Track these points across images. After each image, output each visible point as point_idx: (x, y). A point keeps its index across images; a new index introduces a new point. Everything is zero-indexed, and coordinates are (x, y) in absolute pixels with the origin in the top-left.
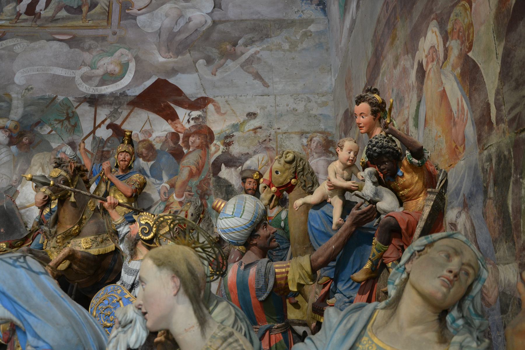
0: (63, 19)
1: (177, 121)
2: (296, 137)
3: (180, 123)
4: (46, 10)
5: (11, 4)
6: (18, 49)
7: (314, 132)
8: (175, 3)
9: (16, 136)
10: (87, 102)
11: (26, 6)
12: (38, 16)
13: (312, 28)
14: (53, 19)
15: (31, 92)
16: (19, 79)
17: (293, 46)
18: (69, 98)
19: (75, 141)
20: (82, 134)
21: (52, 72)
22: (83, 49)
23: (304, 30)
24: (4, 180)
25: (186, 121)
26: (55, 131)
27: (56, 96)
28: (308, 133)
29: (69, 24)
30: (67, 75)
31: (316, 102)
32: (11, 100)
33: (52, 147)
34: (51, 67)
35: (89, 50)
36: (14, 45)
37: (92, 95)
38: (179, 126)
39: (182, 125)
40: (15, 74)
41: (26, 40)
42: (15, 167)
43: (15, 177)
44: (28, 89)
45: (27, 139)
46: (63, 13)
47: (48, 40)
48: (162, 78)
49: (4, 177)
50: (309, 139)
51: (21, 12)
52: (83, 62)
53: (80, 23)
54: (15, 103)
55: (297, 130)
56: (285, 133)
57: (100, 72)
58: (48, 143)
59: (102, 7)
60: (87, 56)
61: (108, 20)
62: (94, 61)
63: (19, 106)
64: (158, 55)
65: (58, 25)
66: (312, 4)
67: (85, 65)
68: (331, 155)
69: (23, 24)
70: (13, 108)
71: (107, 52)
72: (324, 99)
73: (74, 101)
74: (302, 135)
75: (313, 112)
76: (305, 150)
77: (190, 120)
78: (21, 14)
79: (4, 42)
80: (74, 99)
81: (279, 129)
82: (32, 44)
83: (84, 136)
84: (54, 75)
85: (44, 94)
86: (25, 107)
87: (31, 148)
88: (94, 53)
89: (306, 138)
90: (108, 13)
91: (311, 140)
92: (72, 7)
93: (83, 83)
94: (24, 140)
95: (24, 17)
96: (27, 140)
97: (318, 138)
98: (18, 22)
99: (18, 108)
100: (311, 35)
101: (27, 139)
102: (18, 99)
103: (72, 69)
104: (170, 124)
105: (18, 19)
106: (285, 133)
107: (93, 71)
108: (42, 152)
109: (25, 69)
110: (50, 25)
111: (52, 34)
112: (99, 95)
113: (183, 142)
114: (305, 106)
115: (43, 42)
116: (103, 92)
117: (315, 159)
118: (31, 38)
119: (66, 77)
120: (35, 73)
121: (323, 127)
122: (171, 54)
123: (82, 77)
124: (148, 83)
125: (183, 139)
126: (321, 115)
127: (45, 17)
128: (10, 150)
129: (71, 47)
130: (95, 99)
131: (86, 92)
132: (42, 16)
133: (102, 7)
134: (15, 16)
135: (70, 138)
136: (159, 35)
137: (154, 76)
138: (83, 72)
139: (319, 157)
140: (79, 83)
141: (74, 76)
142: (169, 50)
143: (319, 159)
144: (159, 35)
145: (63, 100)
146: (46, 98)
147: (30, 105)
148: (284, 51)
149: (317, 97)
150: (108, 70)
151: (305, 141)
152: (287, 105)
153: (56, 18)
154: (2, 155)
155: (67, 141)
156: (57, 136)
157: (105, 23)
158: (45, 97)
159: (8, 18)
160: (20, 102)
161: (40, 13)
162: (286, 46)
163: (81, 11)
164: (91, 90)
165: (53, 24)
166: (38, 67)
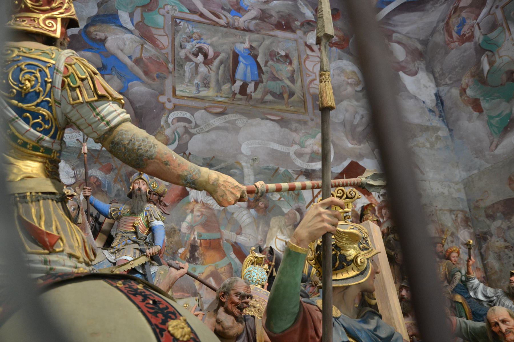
0: (270, 102)
1: (371, 196)
2: (448, 214)
3: (373, 198)
4: (255, 93)
5: (227, 84)
6: (239, 123)
7: (458, 210)
8: (350, 102)
9: (252, 201)
10: (304, 175)
11: (239, 88)
12: (250, 97)
13: (440, 133)
14: (263, 101)
15: (257, 162)
16: (245, 149)
17: (432, 146)
18: (288, 170)
19: (301, 208)
20: (305, 203)
21: (271, 147)
22: (291, 129)
23: (436, 134)
24: (251, 240)
25: (377, 197)
26: (284, 198)
27: (278, 168)
28: (454, 211)
29: (277, 107)
30: (282, 150)
31: (454, 188)
32: (242, 168)
33: (284, 212)
34: (269, 142)
35: (296, 131)
36: (236, 120)
37: (306, 170)
38: (373, 200)
39: (375, 200)
40: (241, 146)
41: (245, 116)
42: (258, 228)
43: (260, 238)
44: (254, 160)
45: (262, 204)
46: (269, 97)
47: (262, 119)
48: (355, 160)
49: (251, 237)
50: (456, 215)
51: (236, 92)
52: (293, 140)
53: (284, 107)
54: (246, 170)
55: (447, 208)
56: (441, 210)
57: (308, 150)
58: (280, 208)
59: (298, 97)
60: (295, 136)
61: (305, 108)
62: (301, 140)
63: (250, 173)
64: (347, 142)
65: (267, 107)
66: (436, 116)
67: (296, 143)
68: (470, 228)
69: (239, 102)
70: (245, 175)
71: (310, 134)
72: (457, 187)
73: (293, 173)
74: (451, 212)
75: (454, 196)
76: (455, 223)
77: (380, 196)
78: (236, 94)
79: (227, 116)
80: (293, 172)
81: (436, 206)
82: (250, 121)
83: (307, 204)
84: (273, 149)
85: (268, 165)
86: (255, 175)
87: (267, 212)
88: (301, 134)
89: (454, 214)
90: (304, 102)
91: (457, 216)
92: (276, 93)
93: (297, 159)
94: (260, 204)
95: (238, 96)
96: (263, 205)
97: (460, 215)
98: (235, 100)
99: (249, 175)
100: (440, 139)
101: (262, 204)
102: (248, 168)
103: (286, 146)
104: (367, 198)
105: (234, 98)
106: (441, 210)
107: (303, 149)
108: (277, 216)
109: (248, 142)
110: (260, 106)
111: (264, 114)
112: (312, 170)
113: (379, 213)
114: (448, 191)
115: (258, 120)
116: (314, 168)
117: (462, 230)
118: (249, 115)
119: (283, 152)
120: (257, 146)
121: (461, 207)
122: (355, 142)
123: (295, 153)
124: (346, 164)
125: (378, 211)
126: (459, 198)
127: (255, 99)
128: (250, 213)
129: (282, 127)
130: (309, 173)
131: (301, 166)
132: (253, 97)
133: (298, 96)
134: (232, 95)
135: (296, 205)
136: (344, 125)
137: (348, 158)
138: (295, 149)
139: (464, 229)
140: (294, 158)
141: (288, 151)
142: (354, 139)
143: (464, 230)
144: (344, 125)
145: (284, 172)
146: (271, 169)
147: (259, 174)
148: (427, 148)
149: (454, 185)
150: (314, 150)
151: (453, 217)
152: (438, 189)
153: (264, 100)
154: (245, 217)
155: (295, 208)
156: (286, 203)
157: (303, 110)
158: (270, 168)
159: (226, 96)
160: (250, 170)
161: (251, 95)
162: (428, 145)
163: (283, 98)
164: (305, 165)
165: (263, 106)
166: (259, 141)
